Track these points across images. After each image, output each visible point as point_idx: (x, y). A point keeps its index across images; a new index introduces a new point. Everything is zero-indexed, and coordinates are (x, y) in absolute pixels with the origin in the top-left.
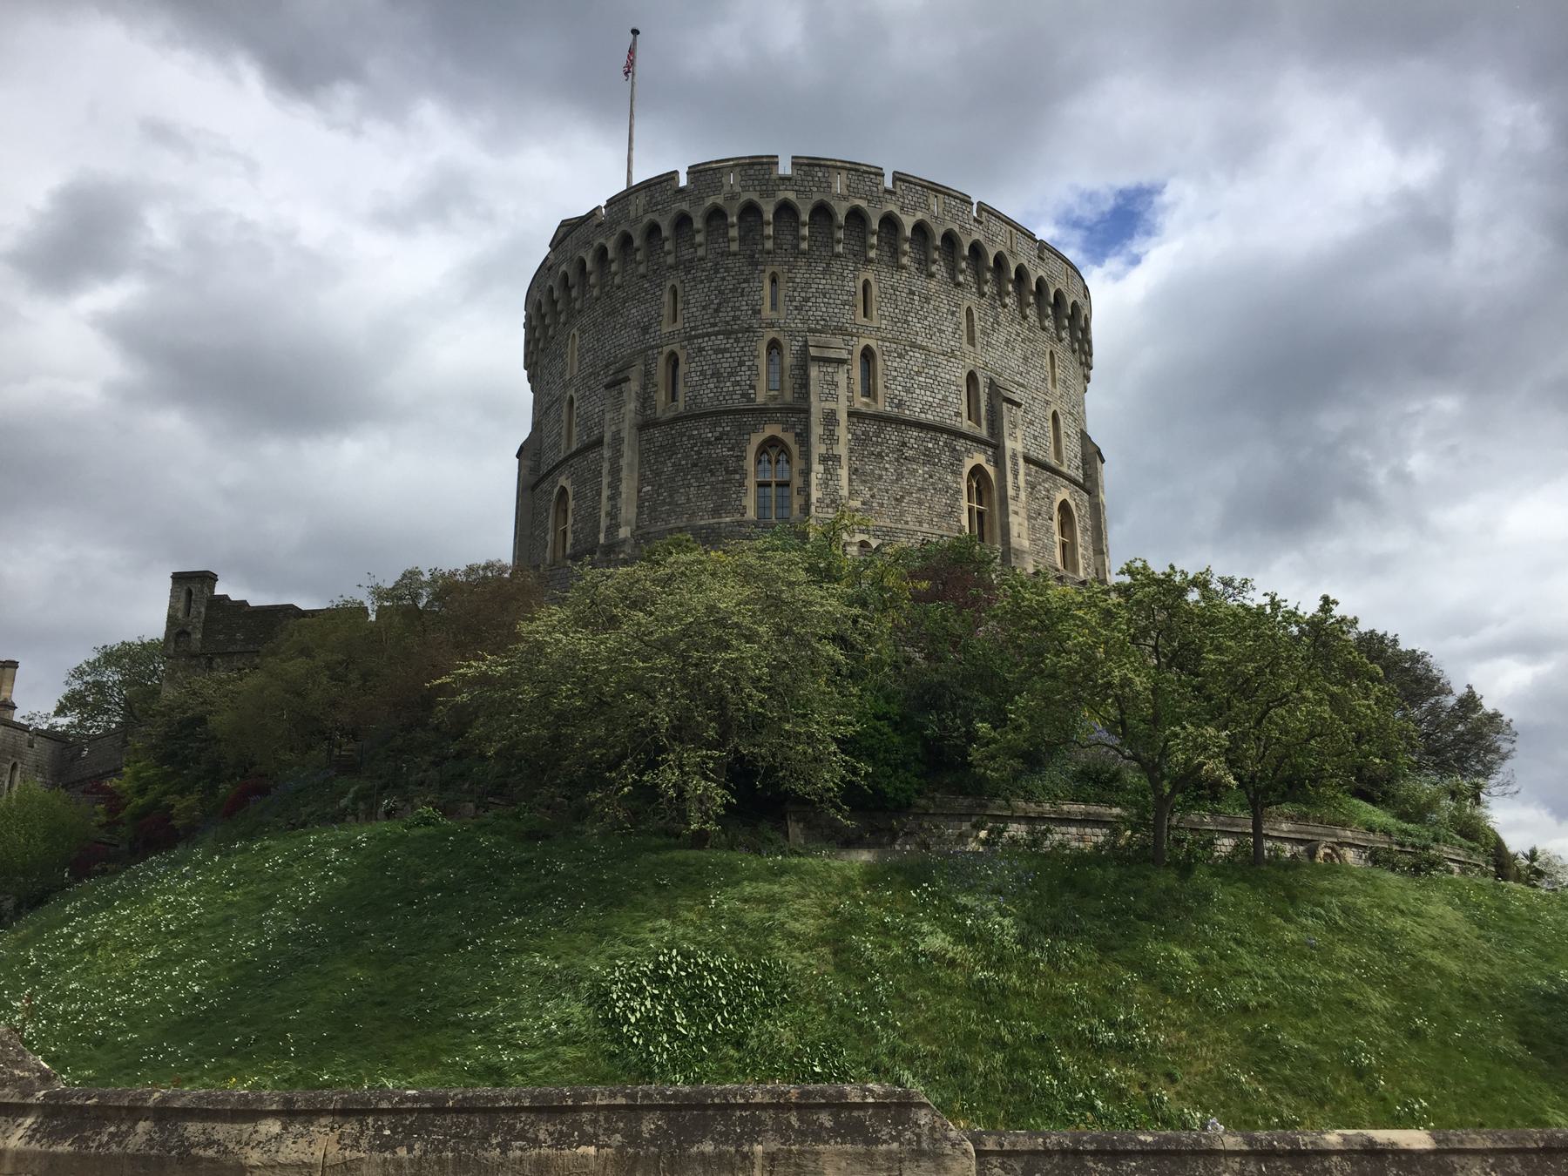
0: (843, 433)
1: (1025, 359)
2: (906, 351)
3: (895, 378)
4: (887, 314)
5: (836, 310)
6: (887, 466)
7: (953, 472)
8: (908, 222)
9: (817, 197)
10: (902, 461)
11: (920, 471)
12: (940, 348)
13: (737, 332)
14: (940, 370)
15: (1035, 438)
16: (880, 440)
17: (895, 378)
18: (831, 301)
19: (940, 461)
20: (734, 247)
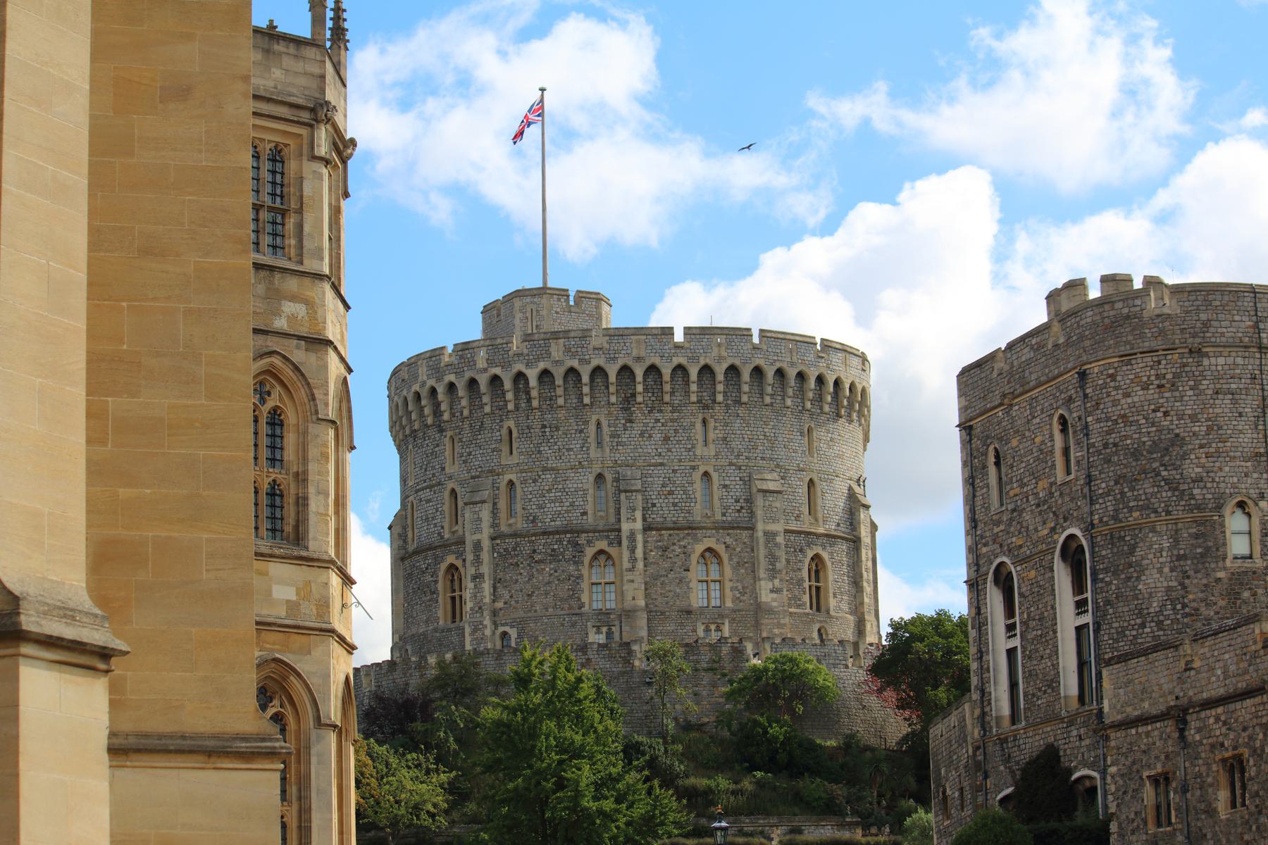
0: (485, 556)
1: (666, 439)
2: (539, 476)
3: (530, 500)
4: (524, 450)
5: (488, 458)
6: (522, 571)
7: (576, 563)
8: (532, 375)
9: (468, 375)
10: (533, 565)
11: (547, 569)
12: (568, 464)
13: (433, 486)
14: (568, 482)
15: (675, 505)
16: (516, 553)
17: (530, 500)
18: (485, 451)
19: (564, 557)
20: (430, 421)
